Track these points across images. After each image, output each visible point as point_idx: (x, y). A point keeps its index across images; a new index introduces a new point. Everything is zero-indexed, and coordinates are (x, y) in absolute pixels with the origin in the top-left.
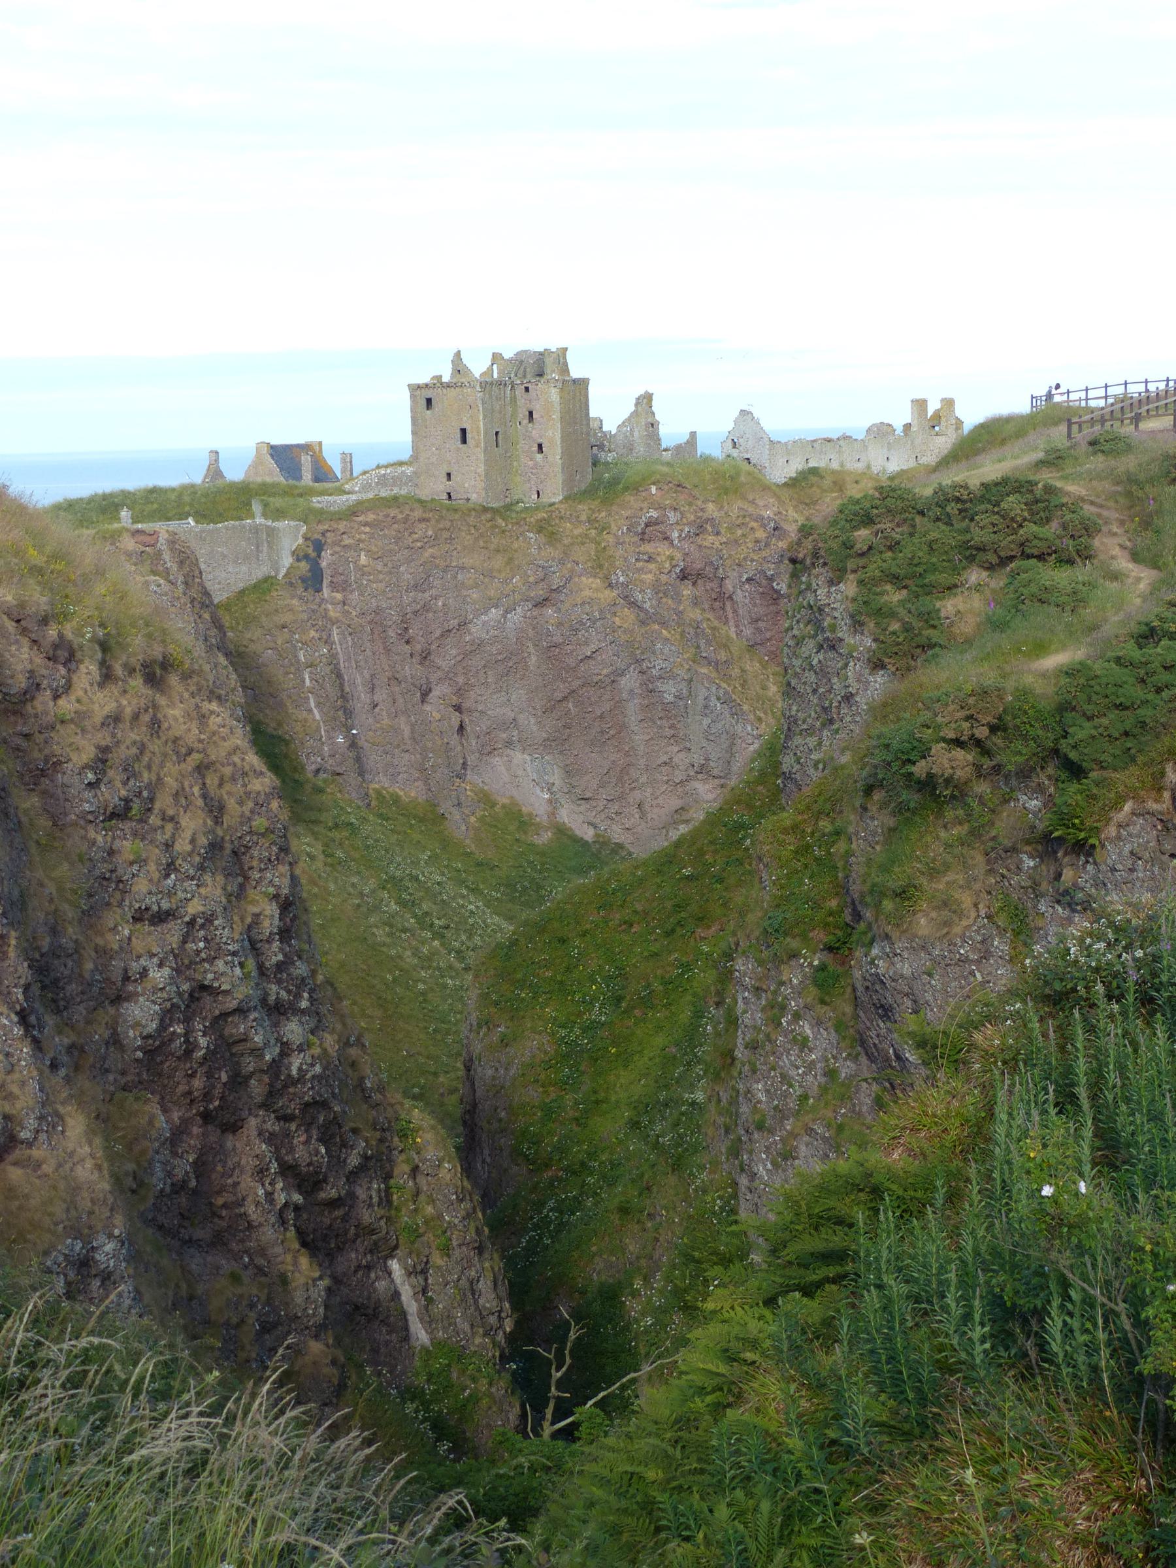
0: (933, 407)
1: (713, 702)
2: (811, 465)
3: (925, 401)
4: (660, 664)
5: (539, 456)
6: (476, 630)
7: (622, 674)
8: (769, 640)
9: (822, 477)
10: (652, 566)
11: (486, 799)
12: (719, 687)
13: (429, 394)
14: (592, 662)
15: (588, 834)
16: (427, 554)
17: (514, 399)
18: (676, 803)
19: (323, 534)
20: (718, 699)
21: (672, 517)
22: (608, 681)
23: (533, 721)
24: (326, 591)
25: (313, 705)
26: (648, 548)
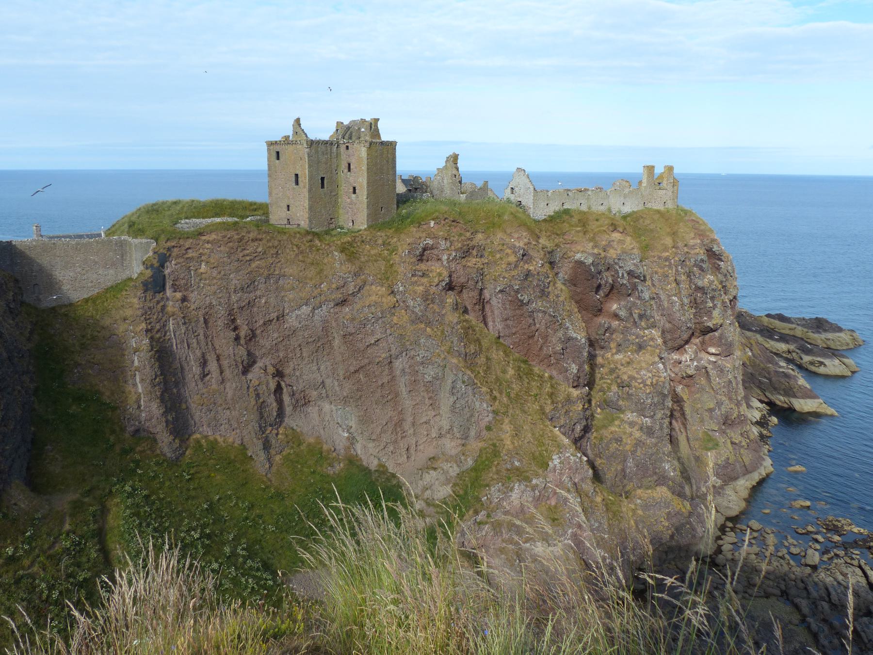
0: (659, 170)
1: (459, 384)
2: (565, 207)
3: (653, 167)
4: (422, 353)
5: (354, 196)
6: (292, 321)
7: (397, 358)
8: (514, 334)
9: (572, 217)
11: (295, 438)
13: (278, 148)
15: (373, 465)
16: (254, 265)
17: (338, 155)
19: (169, 249)
20: (464, 382)
21: (443, 244)
22: (386, 362)
23: (336, 383)
24: (169, 292)
25: (138, 380)
26: (423, 266)
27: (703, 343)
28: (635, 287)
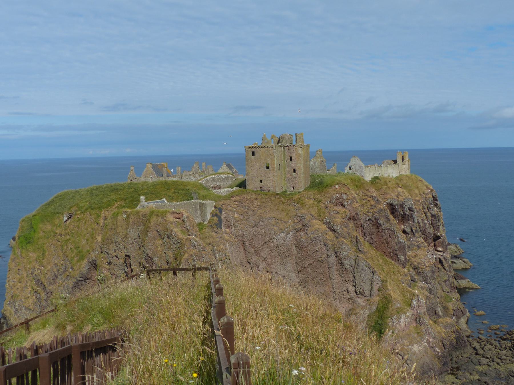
1: (365, 268)
10: (339, 215)
12: (367, 262)
13: (253, 150)
14: (318, 253)
18: (350, 306)
20: (366, 266)
27: (435, 245)
28: (412, 216)
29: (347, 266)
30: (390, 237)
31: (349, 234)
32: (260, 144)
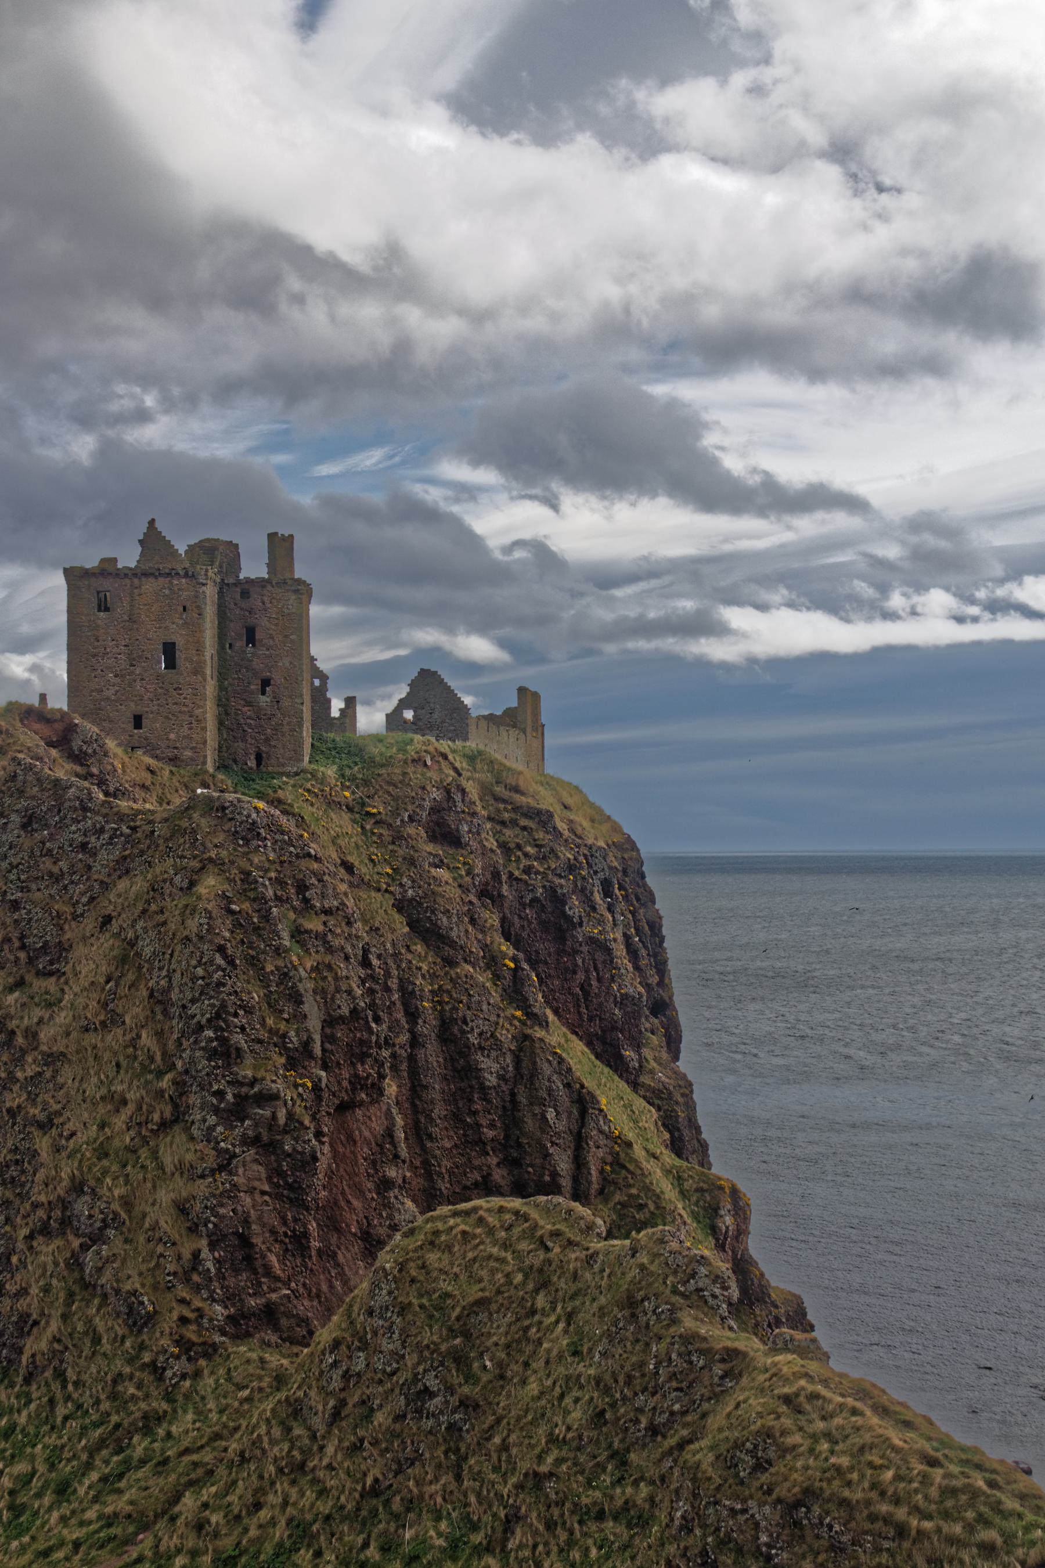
29: (492, 1080)
30: (599, 979)
31: (485, 947)
32: (129, 557)
